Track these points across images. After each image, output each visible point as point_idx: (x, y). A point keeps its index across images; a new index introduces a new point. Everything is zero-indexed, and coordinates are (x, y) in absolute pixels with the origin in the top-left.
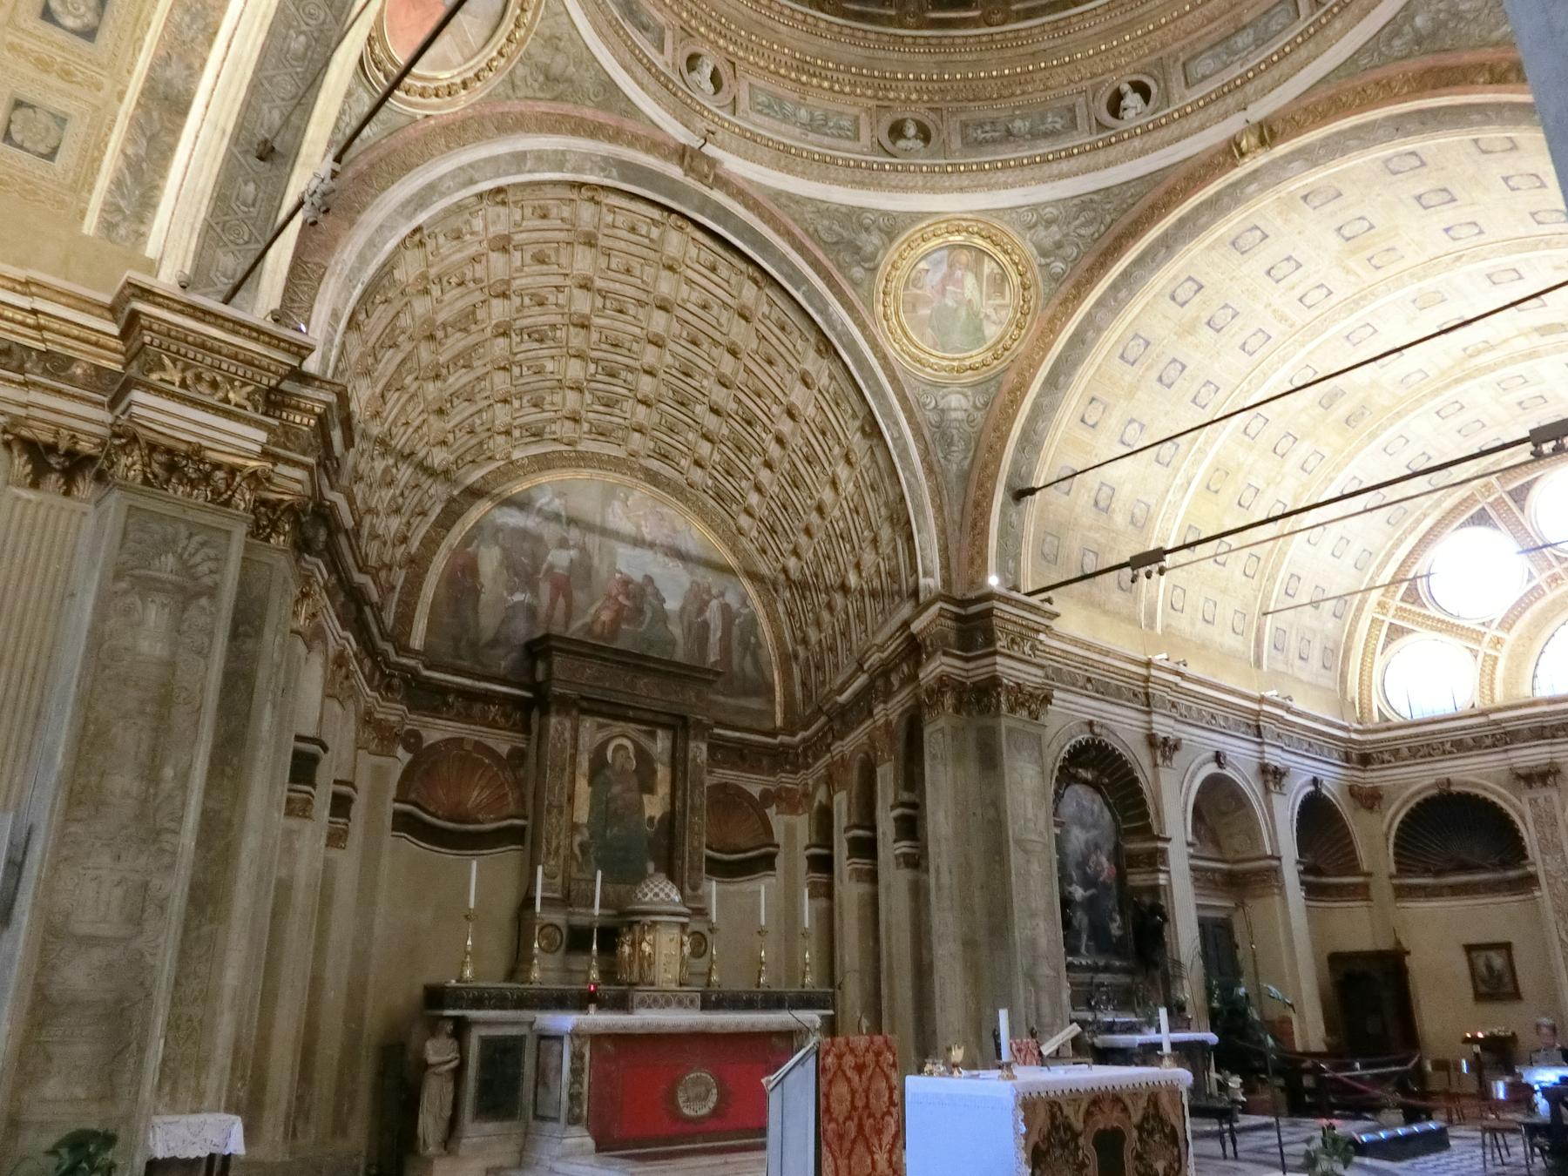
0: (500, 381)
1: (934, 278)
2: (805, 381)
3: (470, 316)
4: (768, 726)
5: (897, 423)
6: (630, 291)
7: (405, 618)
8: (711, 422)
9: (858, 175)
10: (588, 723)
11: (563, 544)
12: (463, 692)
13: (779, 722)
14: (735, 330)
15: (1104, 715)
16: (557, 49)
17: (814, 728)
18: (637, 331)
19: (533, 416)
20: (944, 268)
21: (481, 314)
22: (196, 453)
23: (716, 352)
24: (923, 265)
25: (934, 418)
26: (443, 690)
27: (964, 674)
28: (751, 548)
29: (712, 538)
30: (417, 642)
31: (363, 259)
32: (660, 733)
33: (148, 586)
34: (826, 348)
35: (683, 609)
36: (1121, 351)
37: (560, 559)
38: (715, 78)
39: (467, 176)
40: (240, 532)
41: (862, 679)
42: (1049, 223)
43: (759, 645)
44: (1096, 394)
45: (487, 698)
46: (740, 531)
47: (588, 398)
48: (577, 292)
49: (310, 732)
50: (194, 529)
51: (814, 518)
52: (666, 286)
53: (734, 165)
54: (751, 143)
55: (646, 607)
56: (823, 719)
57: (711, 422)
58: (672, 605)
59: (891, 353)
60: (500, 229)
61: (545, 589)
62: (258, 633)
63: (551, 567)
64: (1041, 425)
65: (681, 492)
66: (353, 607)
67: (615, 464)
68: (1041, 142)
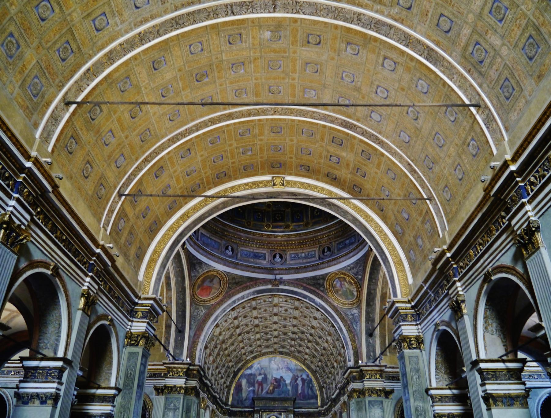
0: (241, 345)
1: (338, 285)
2: (315, 318)
3: (232, 335)
4: (316, 406)
5: (338, 323)
6: (267, 314)
7: (227, 398)
8: (294, 336)
9: (314, 268)
10: (265, 414)
11: (260, 374)
12: (239, 411)
13: (319, 404)
14: (295, 312)
16: (235, 279)
17: (328, 405)
18: (271, 322)
19: (250, 349)
20: (339, 282)
21: (234, 334)
22: (175, 386)
23: (291, 320)
24: (334, 283)
25: (351, 317)
26: (236, 412)
28: (309, 362)
29: (298, 363)
30: (230, 403)
31: (205, 336)
32: (282, 413)
33: (170, 410)
34: (318, 310)
35: (291, 382)
37: (259, 378)
38: (281, 257)
39: (224, 310)
40: (182, 397)
41: (338, 391)
42: (353, 268)
43: (313, 386)
45: (245, 412)
46: (305, 359)
47: (262, 341)
48: (255, 320)
50: (176, 398)
51: (324, 352)
52: (276, 310)
53: (286, 277)
54: (288, 271)
55: (281, 384)
56: (330, 403)
57: (294, 336)
58: (288, 382)
59: (335, 304)
60: (235, 315)
61: (256, 386)
62: (190, 412)
63: (258, 380)
64: (371, 315)
65: (287, 354)
67: (271, 353)
68: (351, 246)
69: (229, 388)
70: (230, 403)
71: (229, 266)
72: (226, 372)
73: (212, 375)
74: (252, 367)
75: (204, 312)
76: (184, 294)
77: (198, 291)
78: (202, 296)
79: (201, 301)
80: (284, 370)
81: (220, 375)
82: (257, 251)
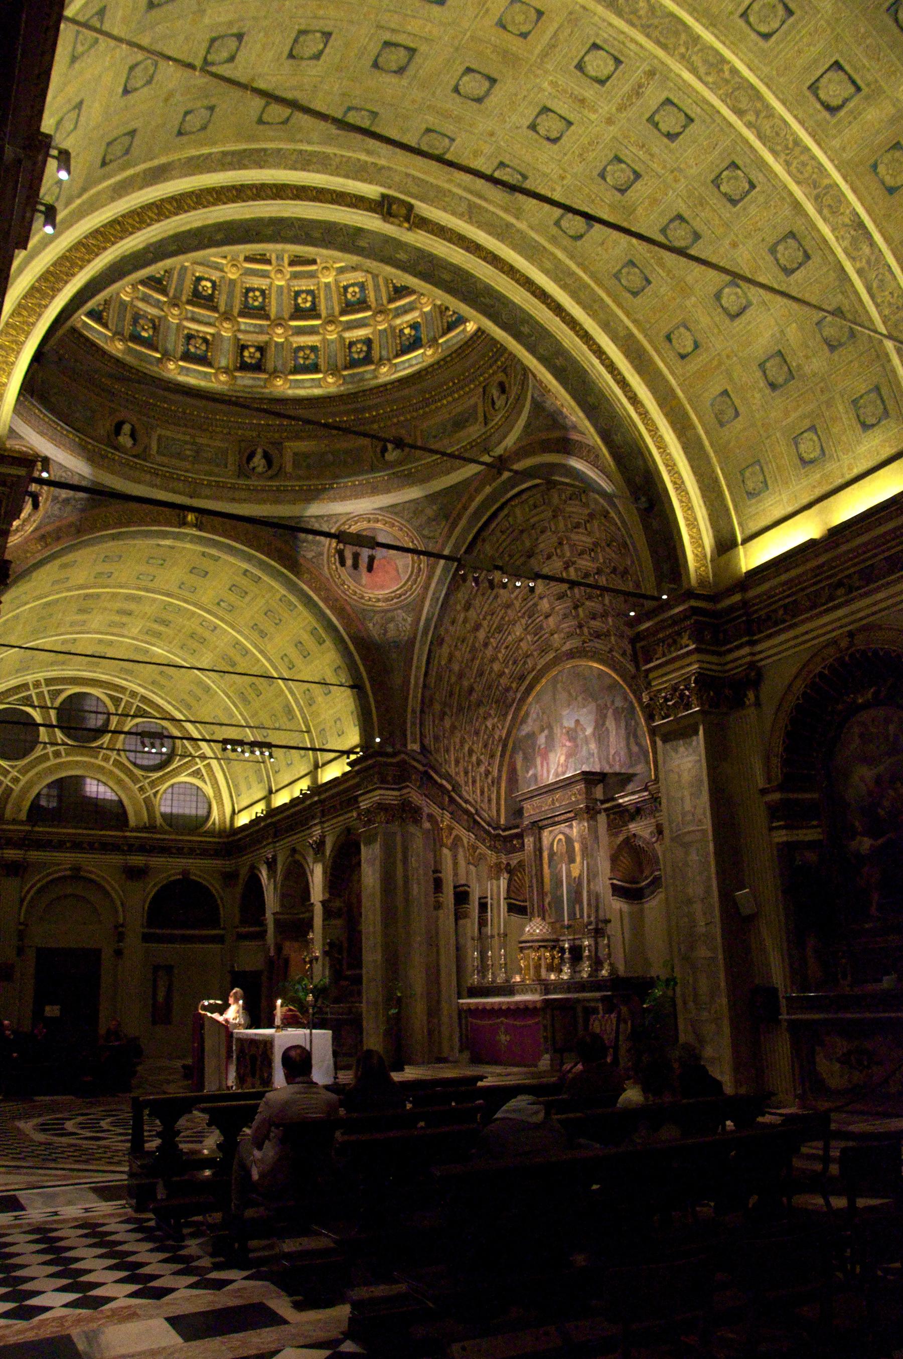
3: (473, 649)
11: (542, 730)
15: (862, 614)
27: (719, 668)
30: (502, 821)
36: (628, 295)
44: (663, 333)
49: (463, 882)
53: (510, 441)
66: (471, 821)
67: (556, 661)
69: (497, 782)
70: (502, 821)
71: (388, 491)
72: (485, 746)
73: (457, 762)
74: (527, 714)
75: (409, 619)
76: (316, 605)
77: (364, 582)
78: (382, 587)
79: (387, 600)
80: (580, 698)
81: (474, 759)
82: (459, 409)
